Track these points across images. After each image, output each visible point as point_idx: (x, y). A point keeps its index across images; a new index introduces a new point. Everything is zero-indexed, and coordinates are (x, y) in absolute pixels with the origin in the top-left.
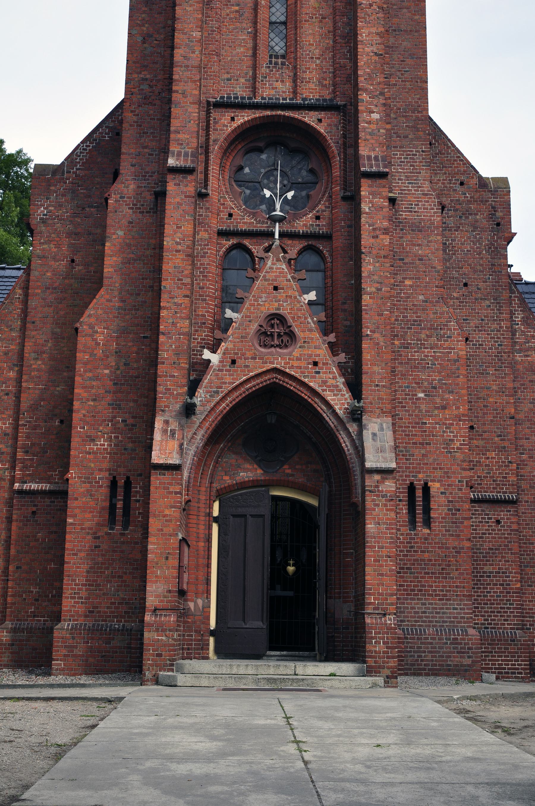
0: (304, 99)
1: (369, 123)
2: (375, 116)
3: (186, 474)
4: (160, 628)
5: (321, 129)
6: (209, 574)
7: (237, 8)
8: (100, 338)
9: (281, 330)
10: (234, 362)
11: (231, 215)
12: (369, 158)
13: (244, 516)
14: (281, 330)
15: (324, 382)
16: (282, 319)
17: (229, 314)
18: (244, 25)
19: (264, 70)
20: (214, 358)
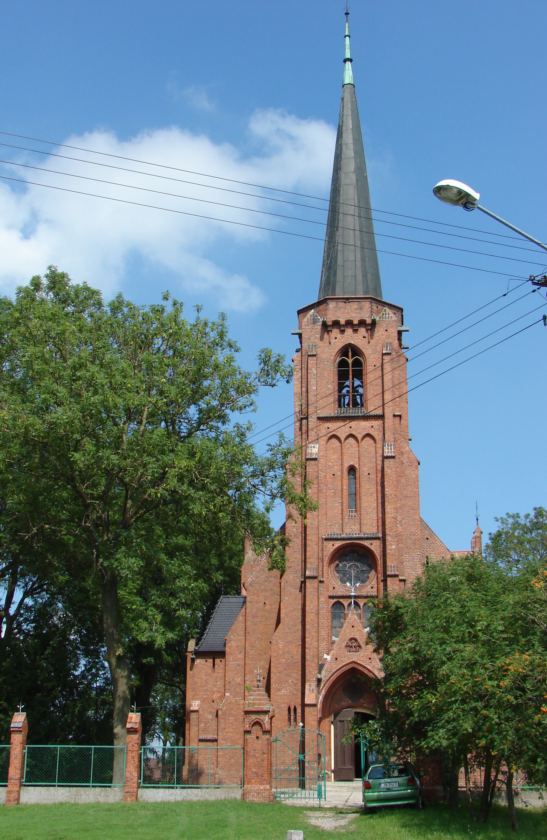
0: (364, 534)
1: (391, 550)
2: (394, 547)
3: (319, 706)
4: (312, 769)
5: (372, 548)
6: (330, 746)
7: (333, 491)
8: (281, 646)
9: (356, 644)
10: (336, 659)
11: (334, 588)
12: (391, 566)
13: (343, 721)
14: (356, 644)
15: (374, 666)
16: (356, 640)
17: (334, 638)
18: (337, 499)
19: (346, 520)
20: (328, 657)
